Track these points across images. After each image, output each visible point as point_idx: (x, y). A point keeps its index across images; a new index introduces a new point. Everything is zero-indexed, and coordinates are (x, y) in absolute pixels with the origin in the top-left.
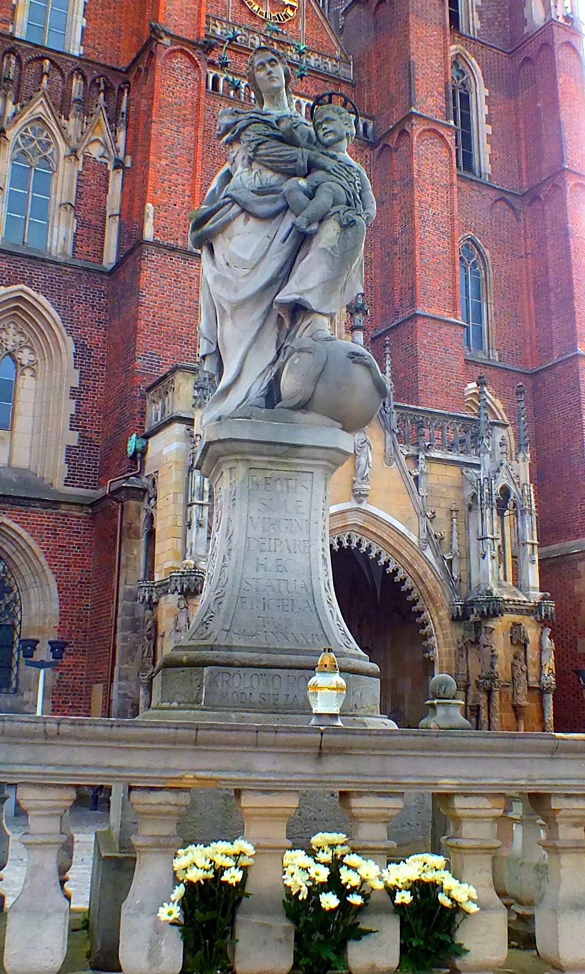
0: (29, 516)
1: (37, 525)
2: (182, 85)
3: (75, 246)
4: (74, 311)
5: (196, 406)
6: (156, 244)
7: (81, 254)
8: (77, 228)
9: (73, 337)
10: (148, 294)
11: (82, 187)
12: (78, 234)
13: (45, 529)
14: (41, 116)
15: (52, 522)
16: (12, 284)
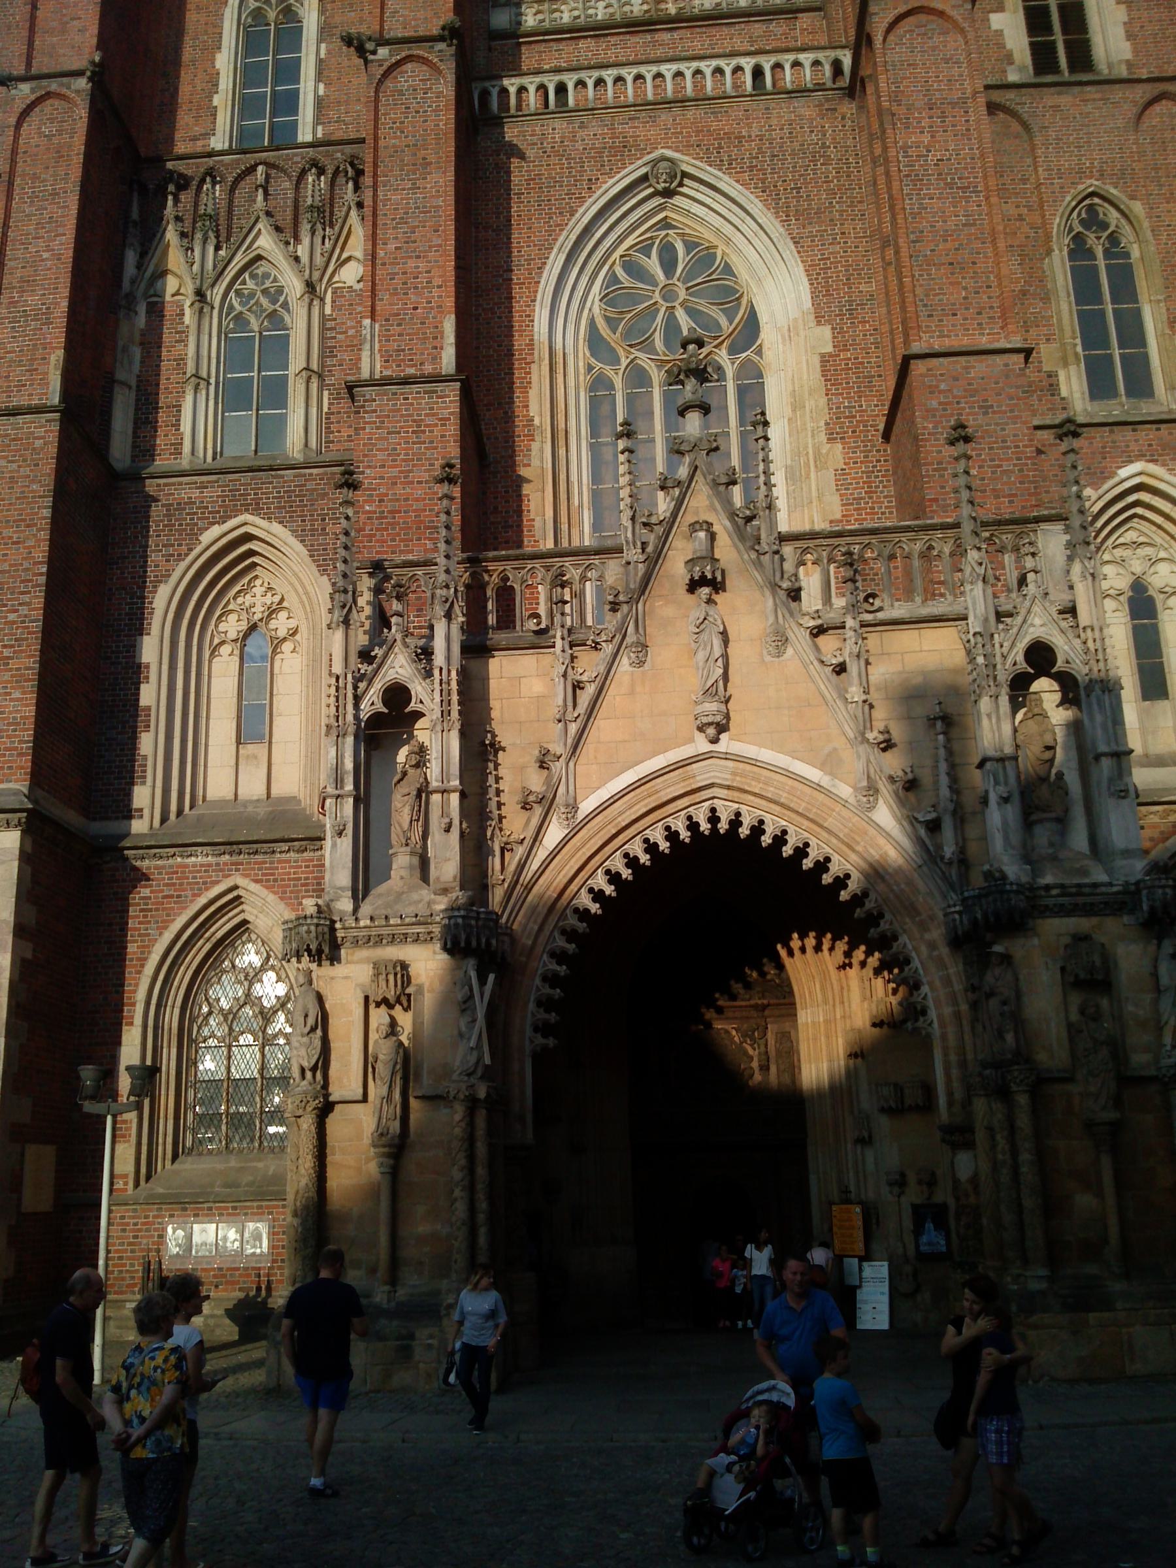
0: (277, 868)
1: (289, 879)
2: (417, 112)
3: (329, 431)
4: (328, 534)
5: (333, 625)
6: (372, 383)
7: (339, 441)
8: (330, 404)
9: (328, 575)
10: (369, 467)
11: (335, 338)
12: (333, 413)
13: (303, 885)
14: (259, 251)
15: (313, 872)
16: (230, 517)
